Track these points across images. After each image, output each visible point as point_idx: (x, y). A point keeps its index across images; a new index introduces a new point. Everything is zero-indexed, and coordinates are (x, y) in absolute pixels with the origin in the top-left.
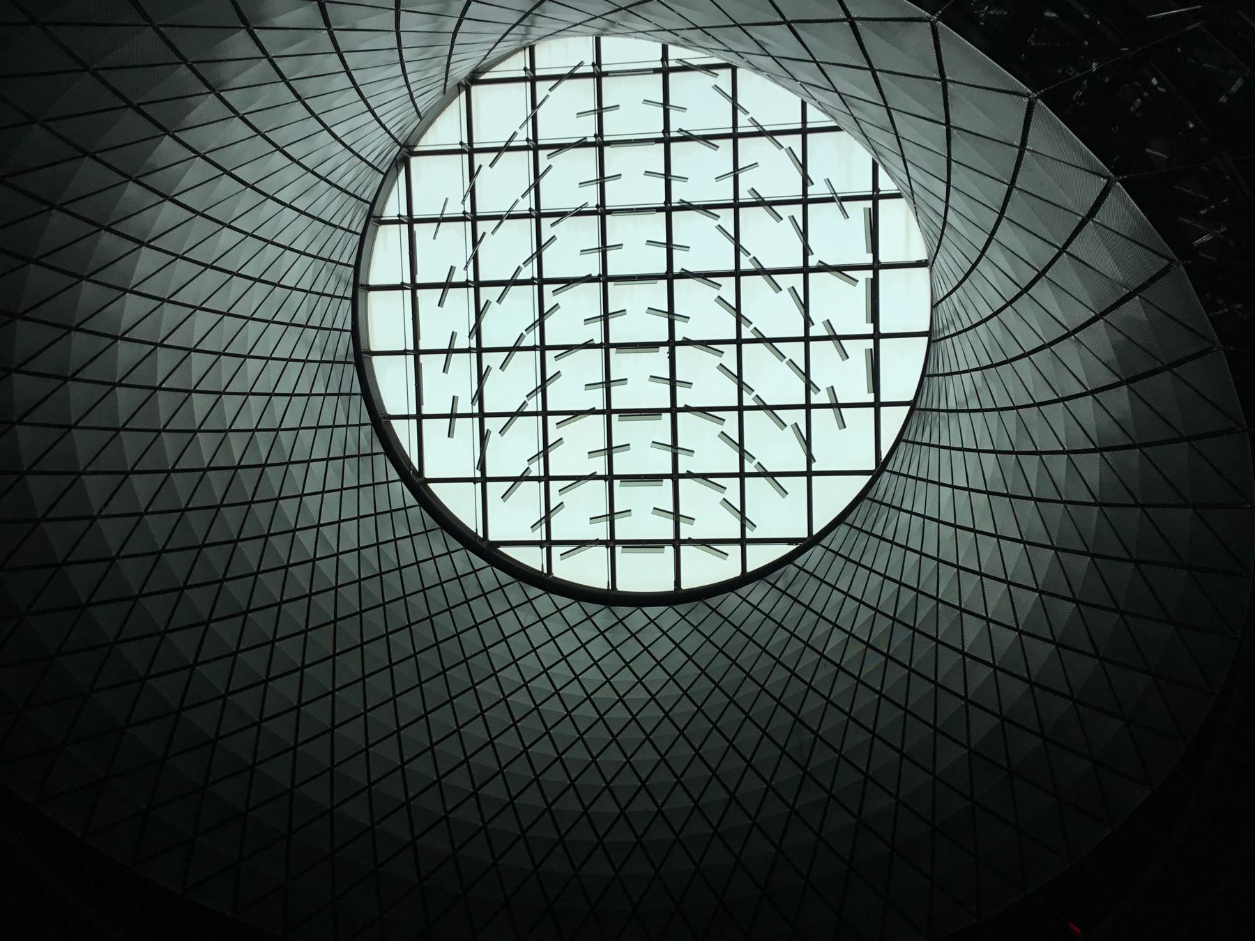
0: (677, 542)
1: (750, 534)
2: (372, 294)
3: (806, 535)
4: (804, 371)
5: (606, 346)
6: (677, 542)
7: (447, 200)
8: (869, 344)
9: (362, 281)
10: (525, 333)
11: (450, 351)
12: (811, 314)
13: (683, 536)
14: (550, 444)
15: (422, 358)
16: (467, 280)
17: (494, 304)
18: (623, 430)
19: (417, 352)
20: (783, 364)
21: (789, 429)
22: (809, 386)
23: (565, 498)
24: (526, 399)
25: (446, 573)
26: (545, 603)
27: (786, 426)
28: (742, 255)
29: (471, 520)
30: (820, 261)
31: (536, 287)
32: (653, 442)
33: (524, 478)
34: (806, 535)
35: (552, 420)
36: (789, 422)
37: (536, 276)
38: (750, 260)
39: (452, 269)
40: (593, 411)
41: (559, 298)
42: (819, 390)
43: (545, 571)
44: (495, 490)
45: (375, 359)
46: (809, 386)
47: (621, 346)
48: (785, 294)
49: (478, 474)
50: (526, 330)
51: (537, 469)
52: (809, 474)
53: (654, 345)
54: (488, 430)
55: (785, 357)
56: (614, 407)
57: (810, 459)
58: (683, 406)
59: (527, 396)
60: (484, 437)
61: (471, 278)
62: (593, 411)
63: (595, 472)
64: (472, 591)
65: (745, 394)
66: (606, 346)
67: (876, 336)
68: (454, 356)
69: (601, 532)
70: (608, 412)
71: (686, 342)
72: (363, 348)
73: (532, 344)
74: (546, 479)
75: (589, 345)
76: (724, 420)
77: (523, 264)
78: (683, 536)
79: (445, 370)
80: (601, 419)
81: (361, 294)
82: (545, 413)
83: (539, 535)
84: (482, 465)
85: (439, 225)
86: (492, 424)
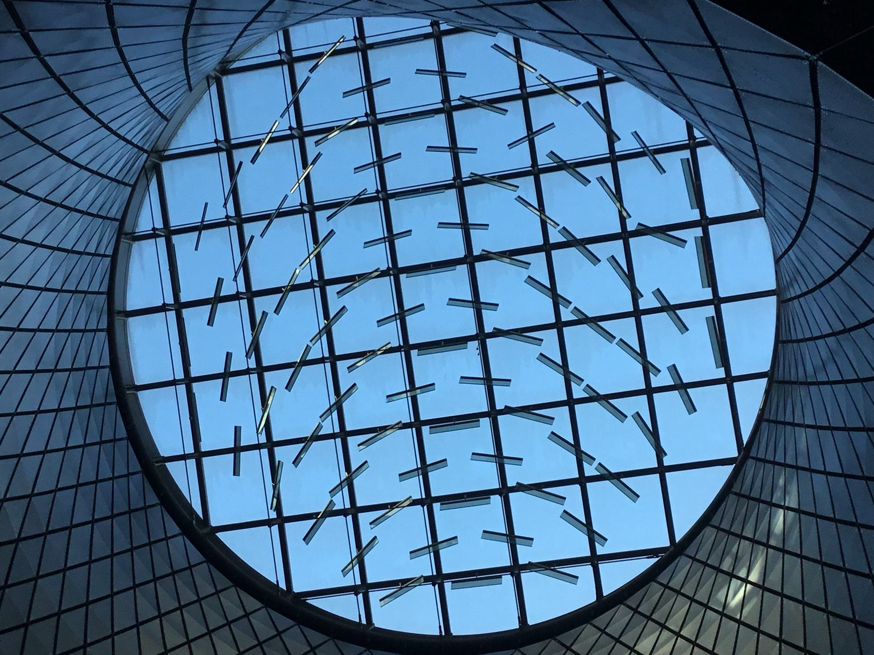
0: (516, 569)
1: (600, 550)
2: (131, 321)
3: (667, 544)
4: (638, 350)
7: (206, 204)
8: (710, 311)
9: (118, 307)
11: (226, 375)
12: (638, 285)
13: (522, 561)
16: (238, 292)
17: (271, 315)
19: (189, 380)
20: (614, 346)
21: (630, 420)
22: (648, 368)
23: (378, 531)
27: (626, 417)
28: (550, 228)
30: (639, 224)
31: (317, 290)
32: (473, 454)
34: (667, 544)
36: (629, 413)
37: (316, 278)
39: (220, 282)
41: (346, 300)
42: (659, 371)
43: (364, 622)
45: (143, 396)
46: (648, 368)
47: (426, 347)
48: (605, 265)
49: (273, 515)
52: (661, 470)
54: (279, 462)
55: (614, 338)
57: (660, 453)
61: (243, 289)
65: (573, 384)
67: (717, 301)
68: (231, 380)
70: (417, 424)
71: (498, 333)
72: (125, 381)
78: (522, 561)
79: (223, 398)
81: (118, 320)
82: (344, 434)
83: (352, 579)
86: (284, 454)
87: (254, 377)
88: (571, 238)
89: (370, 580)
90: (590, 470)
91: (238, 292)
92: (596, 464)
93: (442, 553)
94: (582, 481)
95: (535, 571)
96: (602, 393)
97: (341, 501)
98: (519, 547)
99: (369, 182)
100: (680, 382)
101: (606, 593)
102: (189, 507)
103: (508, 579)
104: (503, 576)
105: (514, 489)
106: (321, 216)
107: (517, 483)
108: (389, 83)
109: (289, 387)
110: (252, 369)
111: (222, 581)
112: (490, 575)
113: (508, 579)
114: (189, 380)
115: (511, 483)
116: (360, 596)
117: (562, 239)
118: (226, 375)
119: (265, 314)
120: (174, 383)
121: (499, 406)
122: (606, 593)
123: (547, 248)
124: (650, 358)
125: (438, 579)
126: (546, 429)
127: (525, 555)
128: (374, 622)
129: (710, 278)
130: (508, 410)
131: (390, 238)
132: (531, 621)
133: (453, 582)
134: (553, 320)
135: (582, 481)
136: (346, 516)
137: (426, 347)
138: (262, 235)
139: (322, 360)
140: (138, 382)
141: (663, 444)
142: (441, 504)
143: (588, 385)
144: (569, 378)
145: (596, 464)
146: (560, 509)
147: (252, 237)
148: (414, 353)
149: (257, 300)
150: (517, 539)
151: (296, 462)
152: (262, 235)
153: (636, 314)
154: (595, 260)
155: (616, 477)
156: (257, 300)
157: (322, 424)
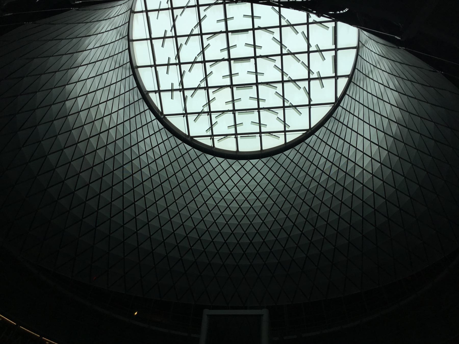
0: (259, 109)
1: (287, 129)
2: (134, 43)
3: (308, 128)
4: (307, 65)
5: (229, 60)
6: (259, 109)
7: (161, 2)
8: (333, 53)
9: (130, 38)
10: (197, 56)
11: (164, 38)
12: (310, 42)
13: (261, 107)
14: (210, 100)
15: (153, 41)
16: (169, 7)
17: (184, 45)
18: (238, 93)
19: (151, 39)
20: (300, 64)
21: (302, 89)
22: (309, 71)
23: (218, 120)
24: (200, 83)
25: (178, 155)
26: (215, 161)
27: (301, 88)
28: (282, 19)
29: (183, 129)
30: (314, 20)
31: (197, 8)
32: (248, 72)
33: (199, 88)
34: (308, 128)
35: (205, 37)
36: (302, 87)
37: (196, 4)
38: (285, 21)
39: (166, 31)
40: (221, 32)
41: (210, 42)
42: (314, 73)
43: (212, 146)
44: (191, 118)
45: (139, 69)
46: (309, 71)
47: (233, 32)
48: (300, 35)
49: (184, 112)
50: (197, 55)
51: (200, 59)
52: (310, 105)
53: (247, 30)
54: (186, 96)
55: (300, 61)
56: (232, 57)
57: (310, 100)
58: (259, 55)
59: (200, 82)
60: (185, 99)
61: (170, 7)
62: (221, 32)
63: (224, 58)
64: (188, 160)
65: (284, 76)
66: (229, 60)
67: (336, 50)
68: (166, 40)
69: (230, 107)
70: (227, 32)
71: (259, 28)
72: (134, 65)
73: (194, 4)
74: (204, 62)
75: (223, 60)
76: (275, 60)
77: (194, 27)
78: (261, 107)
79: (167, 73)
80: (224, 35)
81: (131, 43)
82: (201, 34)
83: (209, 133)
84: (185, 109)
85: (158, 12)
86: (188, 93)
87: (170, 11)
88: (290, 52)
89: (209, 85)
90: (284, 23)
91: (169, 7)
92: (287, 49)
93: (233, 78)
94: (282, 55)
95: (263, 85)
96: (292, 52)
97: (203, 85)
98: (257, 49)
99: (227, 82)
100: (319, 49)
101: (287, 141)
102: (157, 108)
103: (253, 60)
104: (253, 86)
105: (258, 57)
106: (202, 9)
107: (258, 26)
108: (233, 19)
109: (190, 70)
110: (170, 8)
111: (170, 135)
112: (251, 110)
113: (253, 60)
114: (155, 66)
115: (257, 55)
116: (203, 64)
117: (286, 24)
118: (164, 38)
119: (177, 16)
120: (146, 39)
121: (256, 27)
122: (287, 141)
123: (283, 82)
124: (311, 68)
125: (231, 86)
126: (271, 36)
127: (259, 52)
128: (215, 146)
129: (335, 42)
130: (259, 28)
131: (231, 75)
132: (263, 149)
133: (237, 88)
134: (279, 25)
135: (284, 107)
136: (199, 36)
137: (236, 59)
138: (181, 15)
139: (198, 35)
140: (134, 39)
141: (311, 97)
142: (234, 61)
143: (289, 77)
144: (284, 100)
145: (287, 49)
146: (276, 116)
147: (177, 16)
148: (232, 62)
149: (175, 11)
150: (256, 47)
151: (192, 96)
152: (181, 15)
153: (308, 23)
154: (297, 32)
155: (294, 81)
156: (175, 11)
157: (201, 84)
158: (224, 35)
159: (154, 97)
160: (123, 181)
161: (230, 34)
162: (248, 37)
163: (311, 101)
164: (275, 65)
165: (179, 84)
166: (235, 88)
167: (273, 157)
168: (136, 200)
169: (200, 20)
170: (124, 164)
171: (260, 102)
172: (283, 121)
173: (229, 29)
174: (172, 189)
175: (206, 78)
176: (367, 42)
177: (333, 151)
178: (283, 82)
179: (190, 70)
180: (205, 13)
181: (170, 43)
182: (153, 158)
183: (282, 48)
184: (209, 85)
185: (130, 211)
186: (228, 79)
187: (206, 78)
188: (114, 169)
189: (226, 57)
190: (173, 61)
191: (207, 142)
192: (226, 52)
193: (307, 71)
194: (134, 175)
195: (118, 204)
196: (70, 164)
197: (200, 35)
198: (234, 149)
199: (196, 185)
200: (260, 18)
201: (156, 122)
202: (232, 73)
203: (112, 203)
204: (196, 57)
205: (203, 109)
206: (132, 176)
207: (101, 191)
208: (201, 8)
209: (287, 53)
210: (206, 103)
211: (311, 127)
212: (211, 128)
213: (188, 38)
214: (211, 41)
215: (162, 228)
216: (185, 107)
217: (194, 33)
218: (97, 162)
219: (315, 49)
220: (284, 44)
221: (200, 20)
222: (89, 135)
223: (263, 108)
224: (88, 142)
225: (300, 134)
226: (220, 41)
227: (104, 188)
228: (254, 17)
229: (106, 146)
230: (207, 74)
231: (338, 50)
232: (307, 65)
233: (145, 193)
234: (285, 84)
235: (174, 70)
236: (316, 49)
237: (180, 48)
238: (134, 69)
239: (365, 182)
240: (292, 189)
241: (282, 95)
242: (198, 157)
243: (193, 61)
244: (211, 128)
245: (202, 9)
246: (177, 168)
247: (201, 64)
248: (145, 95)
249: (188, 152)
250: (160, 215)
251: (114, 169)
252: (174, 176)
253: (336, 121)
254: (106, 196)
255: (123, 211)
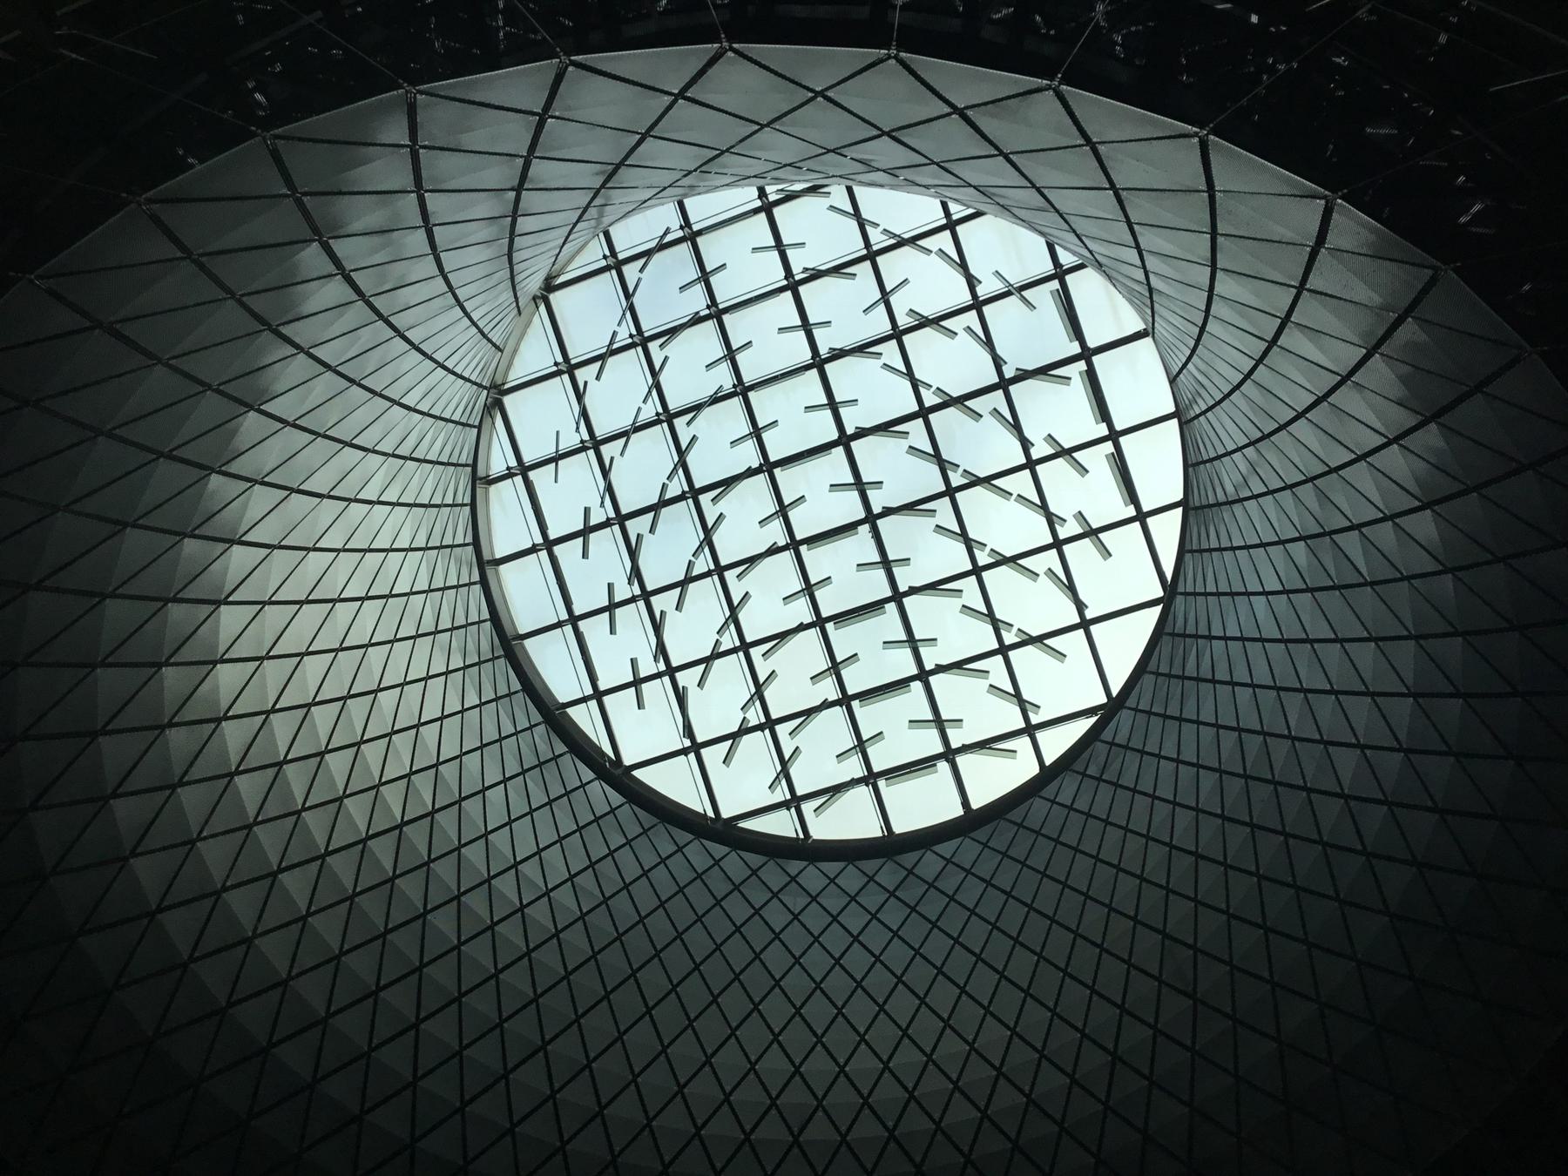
0: (949, 755)
1: (1035, 719)
2: (502, 568)
3: (1104, 700)
4: (1039, 503)
5: (794, 545)
6: (949, 755)
7: (558, 432)
8: (1108, 447)
9: (486, 556)
10: (693, 559)
11: (611, 607)
12: (1027, 433)
13: (955, 745)
15: (582, 624)
17: (647, 537)
18: (844, 639)
19: (574, 620)
20: (1012, 504)
21: (1043, 579)
22: (1051, 519)
23: (799, 740)
24: (717, 637)
25: (684, 876)
26: (812, 877)
27: (1037, 575)
29: (695, 800)
30: (1017, 369)
31: (690, 501)
32: (885, 643)
33: (744, 730)
34: (1104, 700)
36: (1041, 570)
37: (686, 489)
38: (933, 393)
39: (587, 511)
40: (802, 627)
41: (722, 506)
42: (1065, 521)
43: (801, 836)
44: (713, 756)
45: (529, 644)
46: (1051, 519)
47: (812, 540)
49: (687, 743)
50: (693, 556)
52: (1085, 624)
53: (850, 528)
54: (683, 687)
55: (1011, 494)
56: (824, 614)
57: (1080, 606)
58: (907, 589)
59: (718, 633)
60: (681, 698)
61: (612, 514)
62: (802, 627)
63: (826, 699)
64: (721, 888)
65: (976, 552)
66: (794, 545)
67: (1114, 436)
68: (618, 611)
69: (854, 768)
70: (820, 622)
71: (888, 512)
72: (509, 632)
75: (773, 550)
76: (961, 591)
77: (668, 479)
78: (955, 745)
79: (612, 631)
80: (813, 633)
81: (490, 571)
82: (745, 647)
83: (782, 794)
84: (688, 731)
85: (557, 465)
86: (687, 679)
87: (641, 604)
89: (800, 792)
90: (1009, 638)
92: (1014, 630)
93: (869, 751)
94: (1003, 650)
97: (755, 716)
98: (949, 732)
100: (1089, 529)
101: (1048, 762)
103: (943, 766)
106: (679, 423)
107: (936, 665)
109: (679, 607)
110: (638, 596)
113: (943, 766)
114: (574, 620)
116: (793, 810)
117: (938, 401)
118: (611, 607)
119: (639, 537)
120: (559, 625)
122: (1048, 762)
123: (923, 413)
124: (1053, 509)
125: (871, 778)
126: (957, 603)
127: (957, 738)
129: (1104, 414)
130: (913, 591)
131: (757, 433)
133: (886, 779)
135: (1003, 650)
137: (814, 540)
139: (708, 574)
140: (522, 632)
141: (1082, 596)
142: (860, 701)
145: (1014, 630)
147: (612, 459)
150: (945, 723)
151: (701, 684)
158: (813, 633)
159: (585, 719)
160: (495, 976)
161: (803, 549)
162: (861, 546)
163: (1030, 445)
164: (964, 606)
165: (653, 659)
166: (855, 704)
167: (1008, 816)
168: (547, 1037)
169: (682, 453)
170: (495, 919)
171: (948, 731)
172: (1012, 695)
173: (799, 537)
174: (675, 987)
175: (759, 694)
176: (1200, 395)
177: (1207, 733)
178: (923, 413)
179: (679, 607)
180: (692, 430)
181: (632, 618)
182: (597, 892)
183: (1027, 711)
184: (800, 792)
185: (531, 1077)
186: (803, 604)
187: (759, 694)
188: (463, 938)
189: (808, 618)
190: (648, 667)
191: (781, 825)
192: (777, 524)
193: (1044, 519)
194: (533, 955)
195: (484, 1054)
196: (304, 926)
197: (612, 268)
198: (873, 830)
199: (757, 962)
200: (907, 562)
201: (596, 789)
202: (813, 582)
203: (465, 1053)
204: (690, 561)
205: (745, 718)
206: (527, 958)
207: (423, 1015)
208: (753, 651)
209: (1018, 640)
210: (749, 697)
211: (1111, 694)
212: (785, 773)
213: (682, 590)
214: (775, 661)
215: (654, 1123)
216: (686, 723)
217: (669, 495)
218: (397, 917)
219: (1049, 450)
220: (974, 538)
221: (682, 453)
222: (363, 829)
223: (963, 745)
224: (363, 852)
225: (1085, 724)
226: (754, 498)
227: (429, 1005)
228: (892, 564)
229: (427, 864)
230: (761, 680)
231: (1089, 349)
232: (1038, 502)
233: (580, 1011)
234: (960, 497)
235: (632, 618)
236: (1051, 451)
237: (638, 547)
238: (486, 565)
239: (1346, 783)
240: (1113, 905)
241: (1012, 692)
242: (754, 872)
243: (682, 578)
244: (785, 773)
245: (679, 423)
246: (684, 917)
247: (759, 733)
248: (554, 716)
249: (717, 862)
250: (639, 1080)
251: (463, 938)
252: (678, 941)
253: (1203, 686)
254: (441, 1029)
255: (505, 1077)
